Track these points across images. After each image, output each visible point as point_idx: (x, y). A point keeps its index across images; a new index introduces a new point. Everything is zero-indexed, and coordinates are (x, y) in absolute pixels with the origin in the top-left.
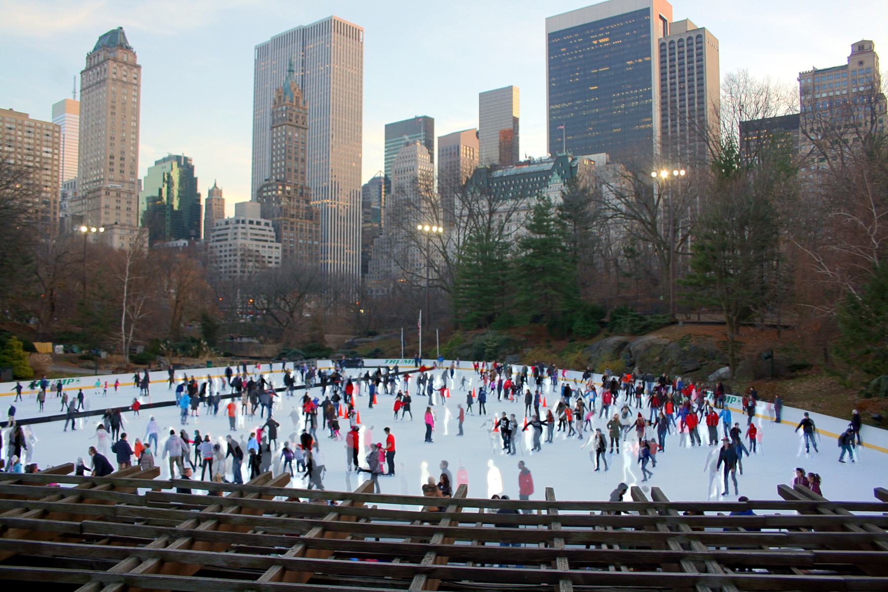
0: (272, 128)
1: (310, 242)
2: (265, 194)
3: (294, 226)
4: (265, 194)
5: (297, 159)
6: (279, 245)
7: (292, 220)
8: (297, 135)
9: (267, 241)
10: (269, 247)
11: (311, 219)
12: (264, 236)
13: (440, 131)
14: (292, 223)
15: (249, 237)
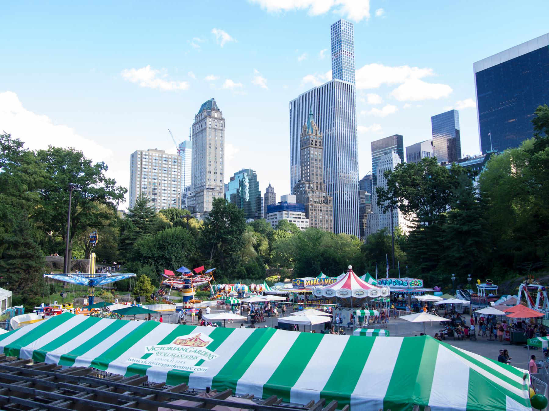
0: (301, 150)
1: (326, 218)
2: (298, 190)
3: (317, 208)
4: (298, 190)
5: (317, 167)
6: (308, 220)
7: (315, 205)
8: (316, 153)
9: (300, 218)
10: (302, 222)
11: (327, 203)
12: (298, 215)
13: (407, 143)
14: (315, 207)
15: (290, 216)
